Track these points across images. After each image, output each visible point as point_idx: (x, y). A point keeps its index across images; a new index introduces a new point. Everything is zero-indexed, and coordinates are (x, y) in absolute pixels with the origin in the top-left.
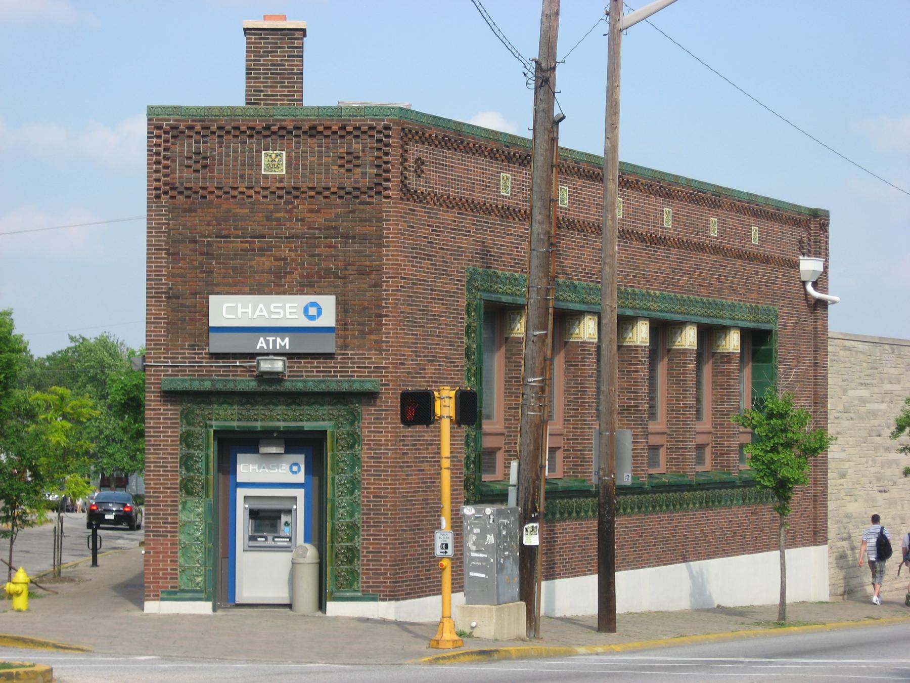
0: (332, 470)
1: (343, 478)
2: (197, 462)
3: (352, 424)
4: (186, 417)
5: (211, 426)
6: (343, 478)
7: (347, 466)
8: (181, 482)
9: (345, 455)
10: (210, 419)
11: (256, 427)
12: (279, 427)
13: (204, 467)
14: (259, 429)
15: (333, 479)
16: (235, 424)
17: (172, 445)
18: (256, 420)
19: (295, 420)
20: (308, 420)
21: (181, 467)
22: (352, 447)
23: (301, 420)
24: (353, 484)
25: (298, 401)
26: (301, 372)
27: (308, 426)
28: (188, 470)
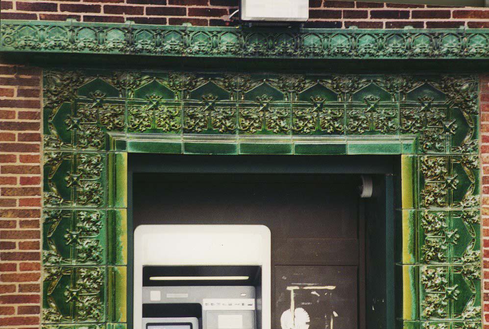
0: (414, 251)
1: (436, 272)
2: (88, 232)
3: (458, 140)
4: (60, 120)
5: (122, 145)
6: (436, 272)
7: (449, 241)
8: (47, 283)
9: (438, 214)
10: (119, 128)
11: (232, 147)
12: (286, 148)
13: (102, 246)
14: (238, 152)
15: (416, 273)
16: (179, 139)
17: (25, 191)
18: (230, 131)
19: (321, 132)
20: (354, 132)
21: (46, 247)
22: (458, 196)
23: (336, 132)
24: (462, 286)
25: (329, 84)
26: (337, 15)
27: (355, 145)
28: (64, 252)
